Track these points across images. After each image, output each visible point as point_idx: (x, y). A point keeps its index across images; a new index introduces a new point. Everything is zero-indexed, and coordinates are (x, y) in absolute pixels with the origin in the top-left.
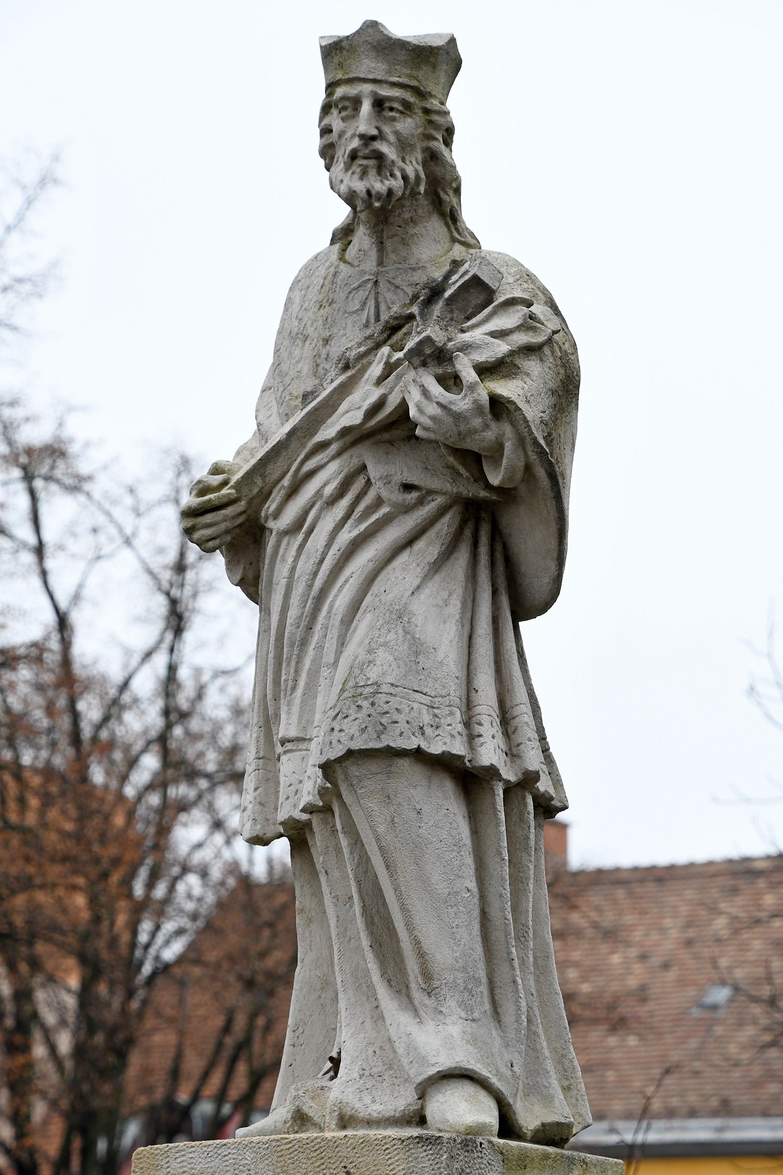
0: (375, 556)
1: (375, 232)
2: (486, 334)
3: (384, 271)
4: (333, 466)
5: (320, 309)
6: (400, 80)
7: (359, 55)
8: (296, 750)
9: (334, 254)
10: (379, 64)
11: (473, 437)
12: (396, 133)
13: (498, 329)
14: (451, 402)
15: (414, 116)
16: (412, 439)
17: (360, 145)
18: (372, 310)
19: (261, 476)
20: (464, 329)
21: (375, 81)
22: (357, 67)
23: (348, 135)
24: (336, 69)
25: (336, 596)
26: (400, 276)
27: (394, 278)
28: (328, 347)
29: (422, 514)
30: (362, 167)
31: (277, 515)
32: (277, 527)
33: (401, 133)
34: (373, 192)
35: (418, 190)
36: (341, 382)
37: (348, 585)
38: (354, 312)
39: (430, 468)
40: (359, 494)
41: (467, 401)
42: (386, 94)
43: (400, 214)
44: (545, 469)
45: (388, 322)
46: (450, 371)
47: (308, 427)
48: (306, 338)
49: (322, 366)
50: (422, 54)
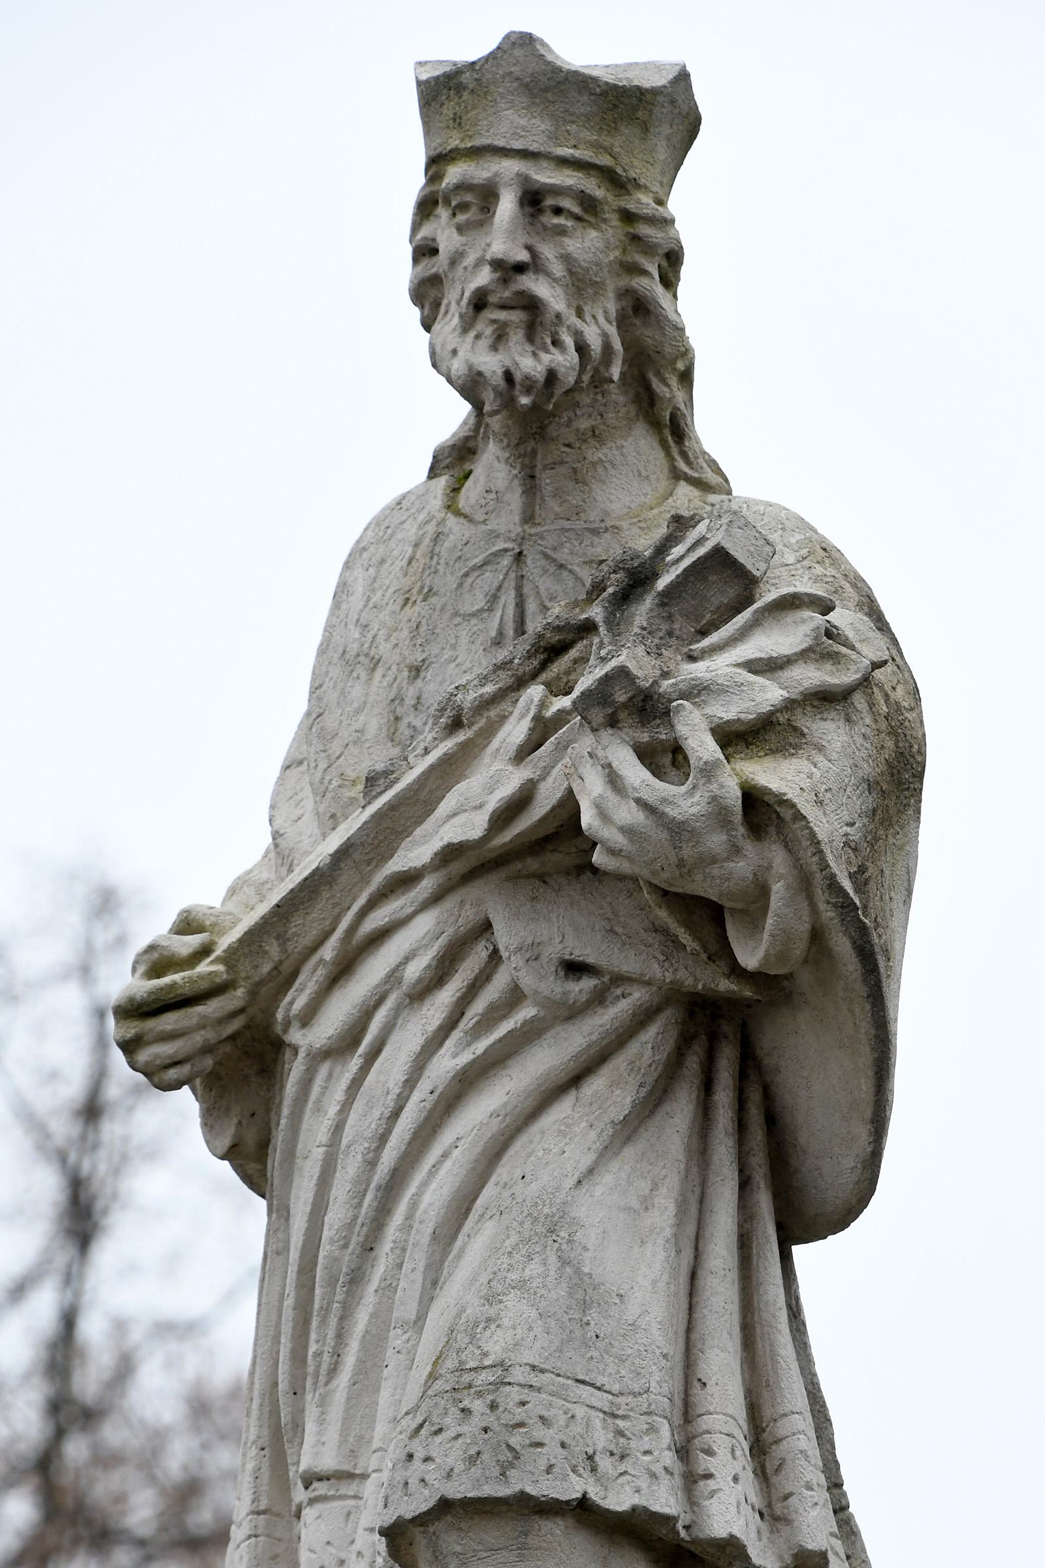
0: (505, 1105)
1: (520, 456)
2: (738, 665)
3: (536, 535)
4: (425, 923)
5: (405, 605)
6: (577, 153)
7: (496, 100)
9: (435, 497)
10: (533, 121)
11: (707, 870)
12: (566, 258)
13: (763, 655)
14: (664, 800)
15: (603, 226)
16: (584, 873)
17: (492, 281)
18: (511, 611)
19: (278, 938)
20: (695, 654)
21: (525, 154)
22: (491, 125)
23: (470, 260)
24: (448, 127)
25: (425, 1184)
26: (567, 545)
27: (555, 549)
28: (419, 683)
29: (600, 1022)
30: (495, 326)
31: (307, 1018)
32: (307, 1042)
33: (575, 260)
34: (518, 377)
35: (607, 375)
36: (445, 754)
37: (448, 1164)
38: (473, 615)
39: (620, 930)
40: (476, 979)
41: (696, 798)
42: (548, 181)
43: (570, 420)
44: (851, 938)
45: (540, 636)
46: (663, 737)
47: (376, 842)
48: (375, 663)
49: (405, 721)
50: (621, 103)
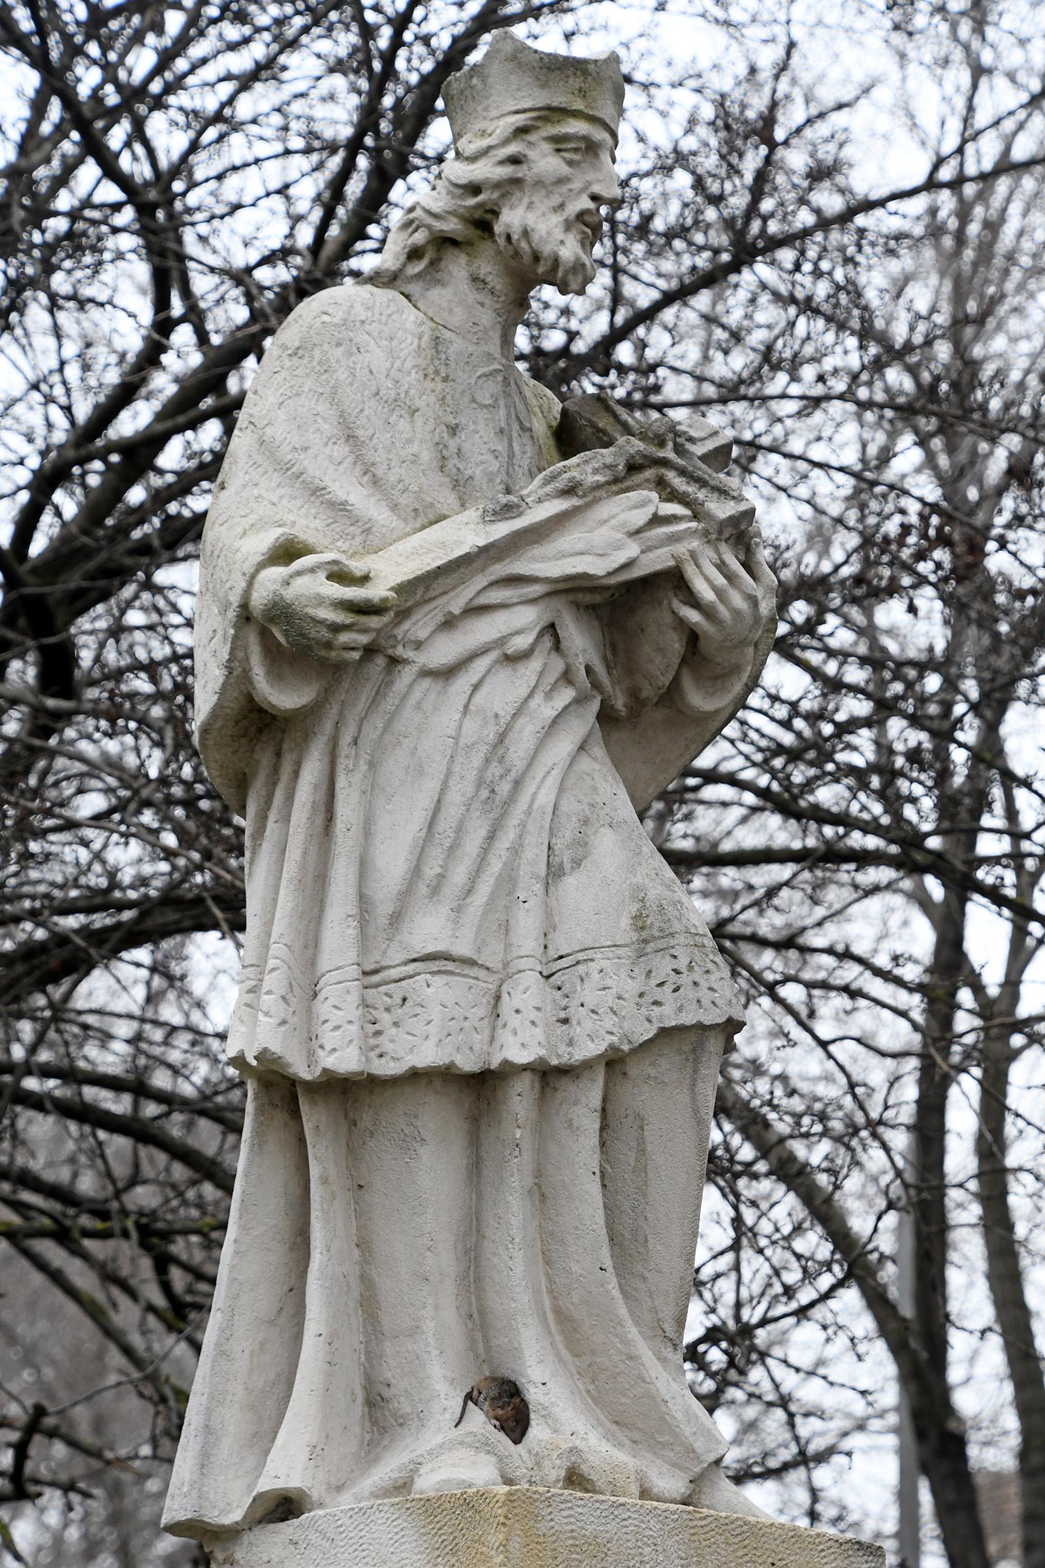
8: (459, 974)
31: (418, 645)
48: (414, 411)
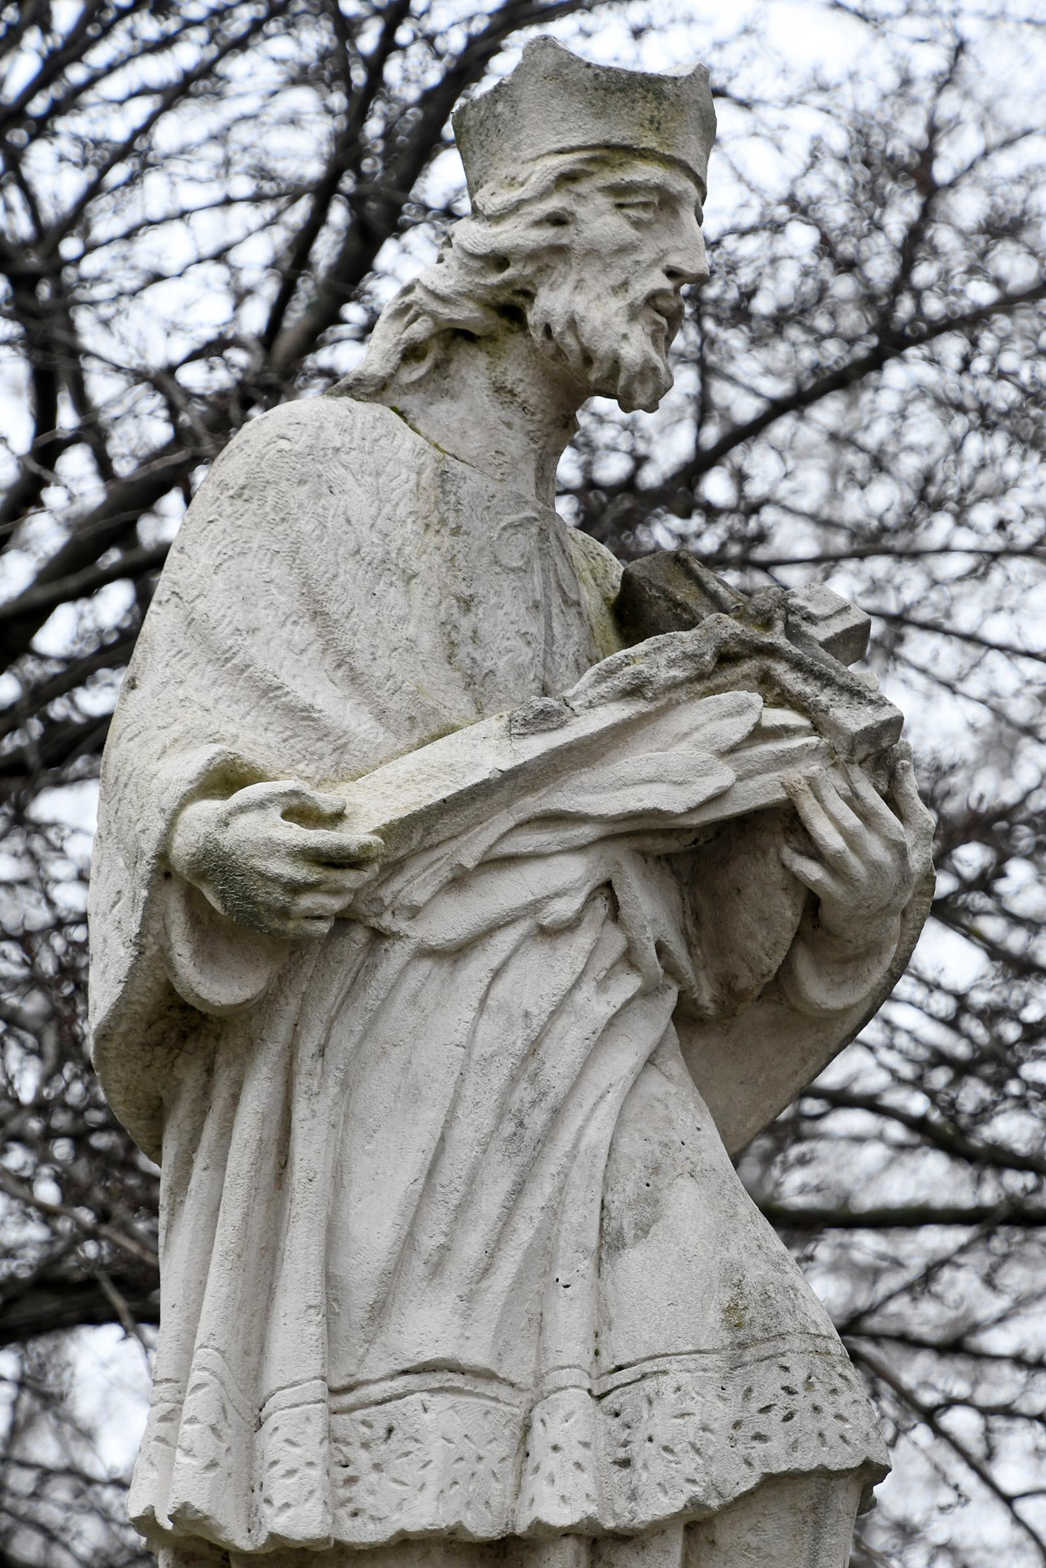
8: (470, 1393)
